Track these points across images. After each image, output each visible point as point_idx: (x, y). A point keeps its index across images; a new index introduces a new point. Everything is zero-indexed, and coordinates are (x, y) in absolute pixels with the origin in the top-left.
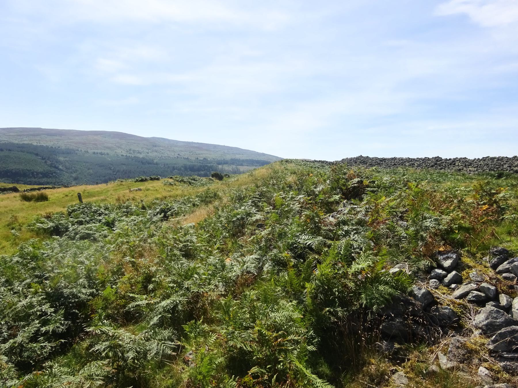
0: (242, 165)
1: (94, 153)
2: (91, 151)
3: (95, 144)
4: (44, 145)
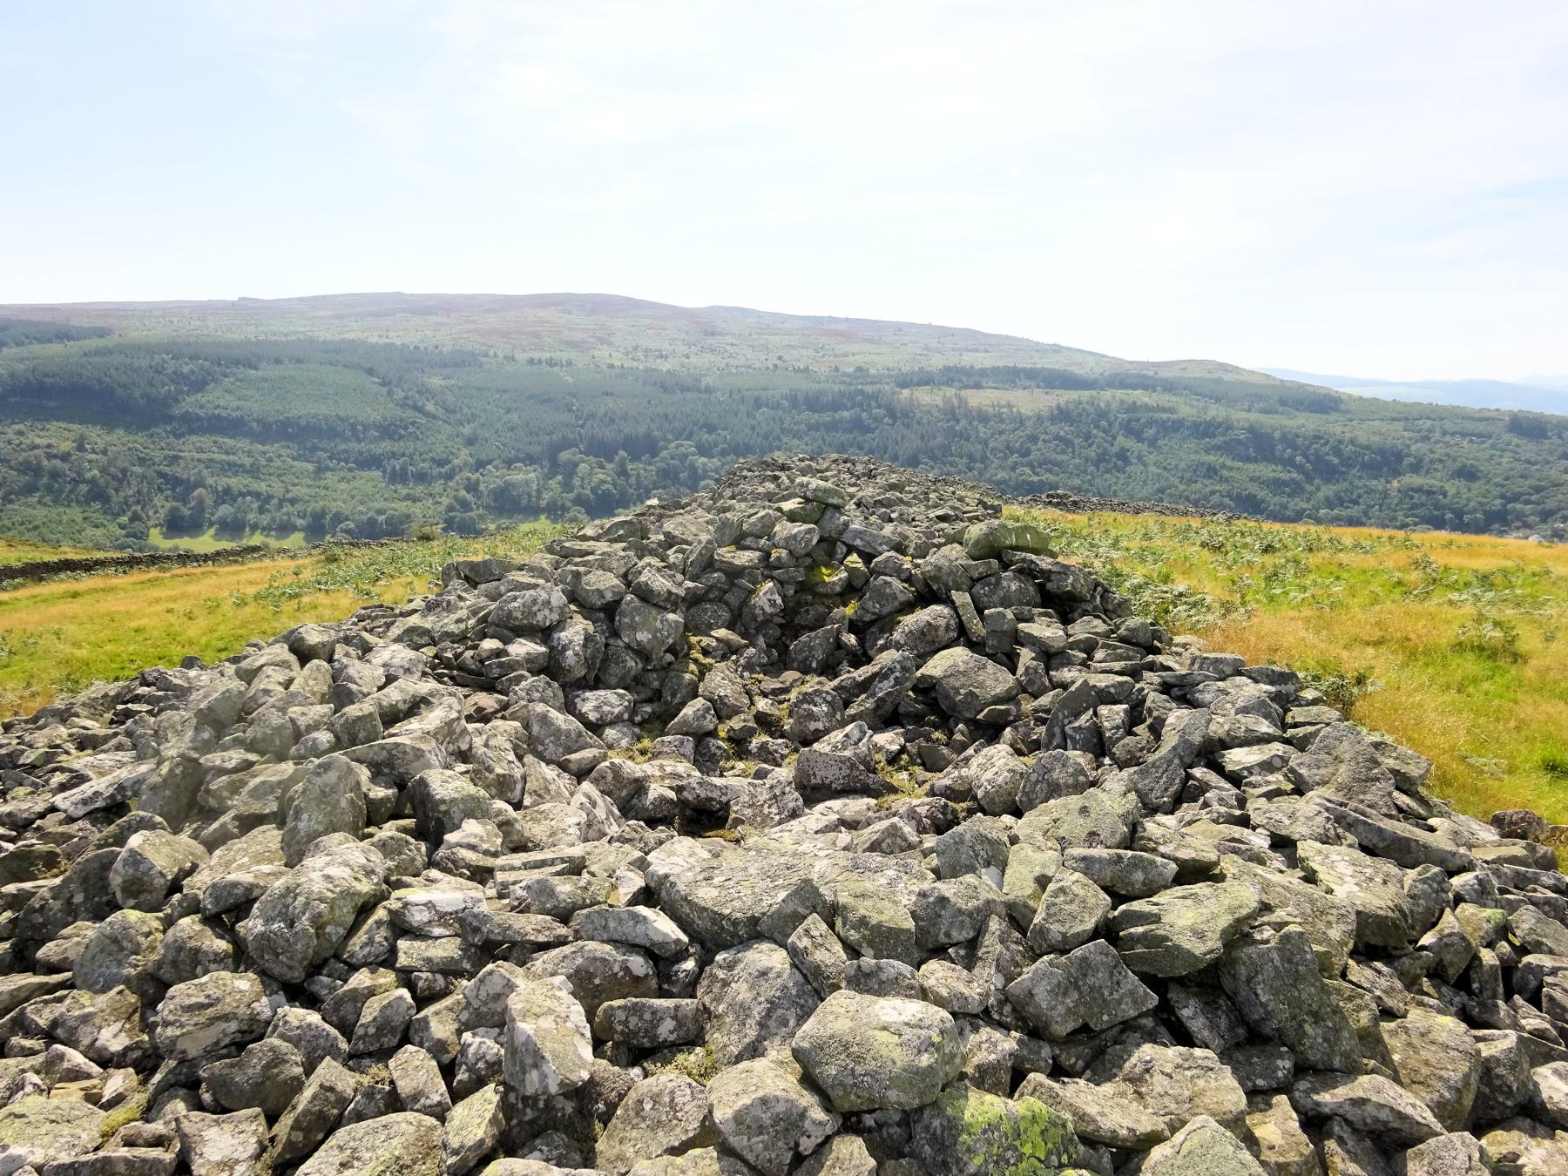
0: (978, 386)
1: (531, 361)
2: (522, 357)
3: (537, 335)
4: (398, 342)
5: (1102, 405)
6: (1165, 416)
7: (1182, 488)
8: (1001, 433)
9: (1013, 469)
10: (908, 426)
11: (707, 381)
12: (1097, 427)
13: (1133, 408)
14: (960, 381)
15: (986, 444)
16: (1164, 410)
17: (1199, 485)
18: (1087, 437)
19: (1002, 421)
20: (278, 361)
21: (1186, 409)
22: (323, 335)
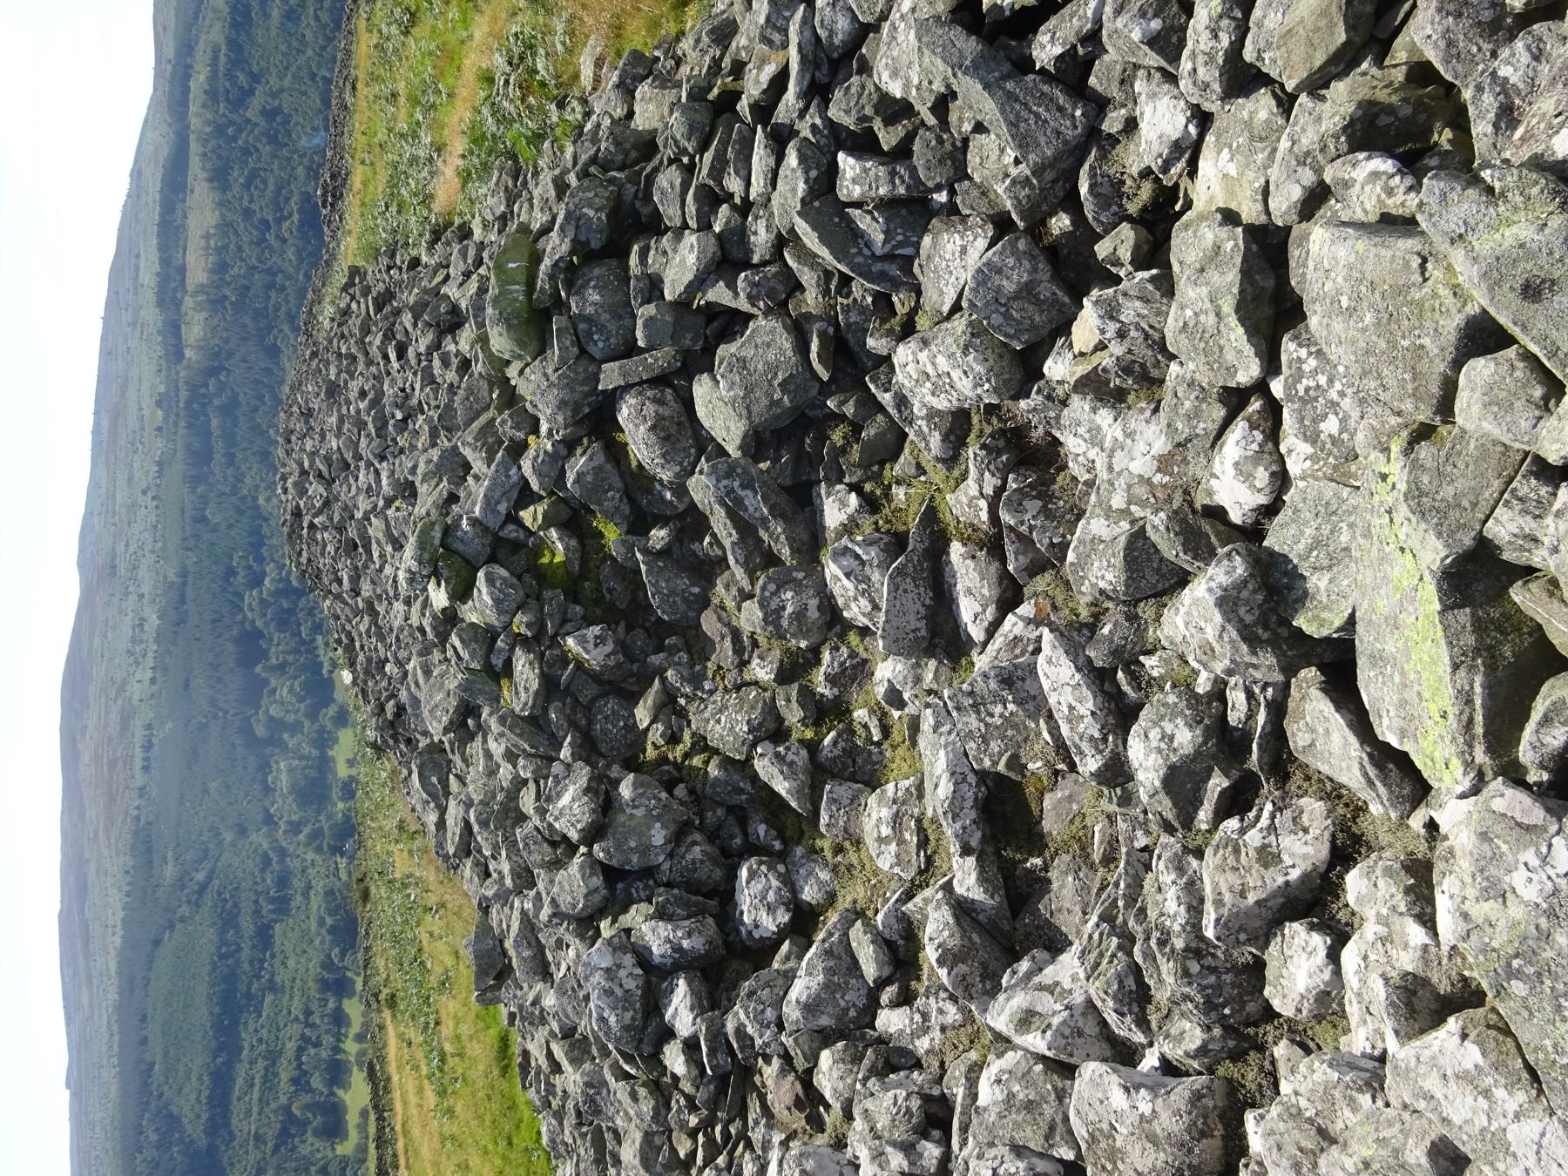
0: (182, 270)
1: (146, 769)
2: (139, 780)
3: (113, 764)
4: (120, 914)
5: (208, 129)
6: (223, 59)
7: (310, 53)
8: (240, 249)
9: (284, 241)
10: (231, 354)
11: (172, 575)
12: (234, 139)
13: (212, 94)
14: (175, 290)
15: (254, 268)
16: (215, 58)
17: (308, 33)
18: (246, 152)
19: (226, 247)
20: (144, 1041)
21: (215, 33)
22: (113, 995)
